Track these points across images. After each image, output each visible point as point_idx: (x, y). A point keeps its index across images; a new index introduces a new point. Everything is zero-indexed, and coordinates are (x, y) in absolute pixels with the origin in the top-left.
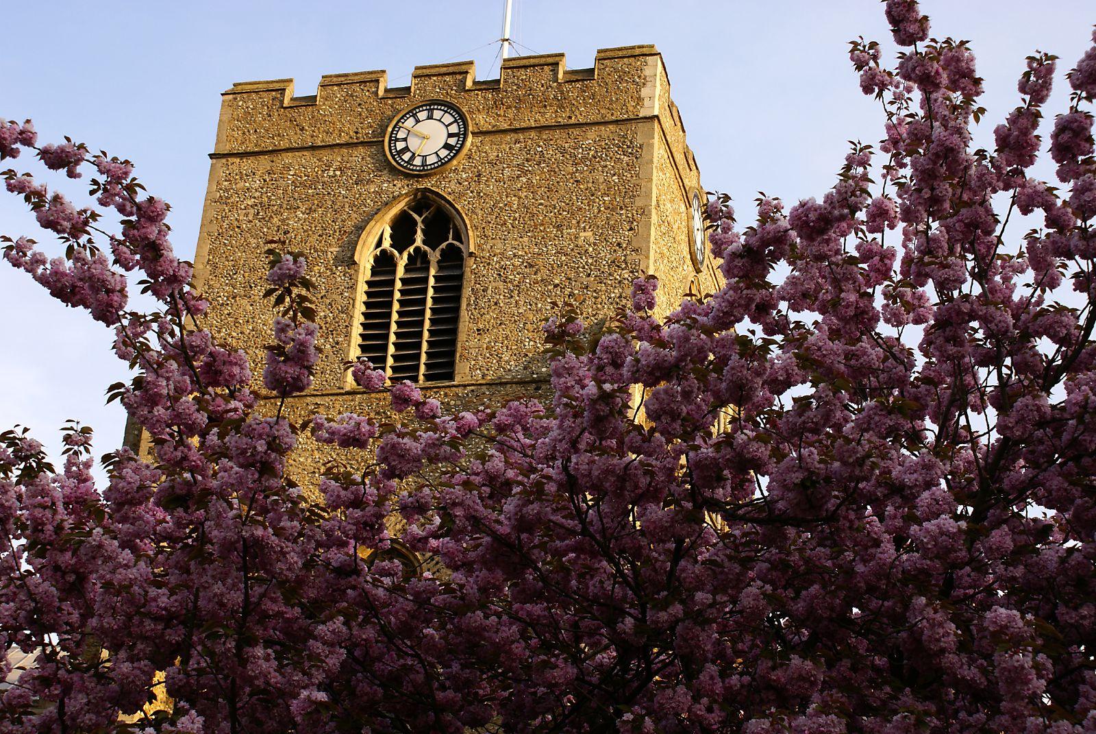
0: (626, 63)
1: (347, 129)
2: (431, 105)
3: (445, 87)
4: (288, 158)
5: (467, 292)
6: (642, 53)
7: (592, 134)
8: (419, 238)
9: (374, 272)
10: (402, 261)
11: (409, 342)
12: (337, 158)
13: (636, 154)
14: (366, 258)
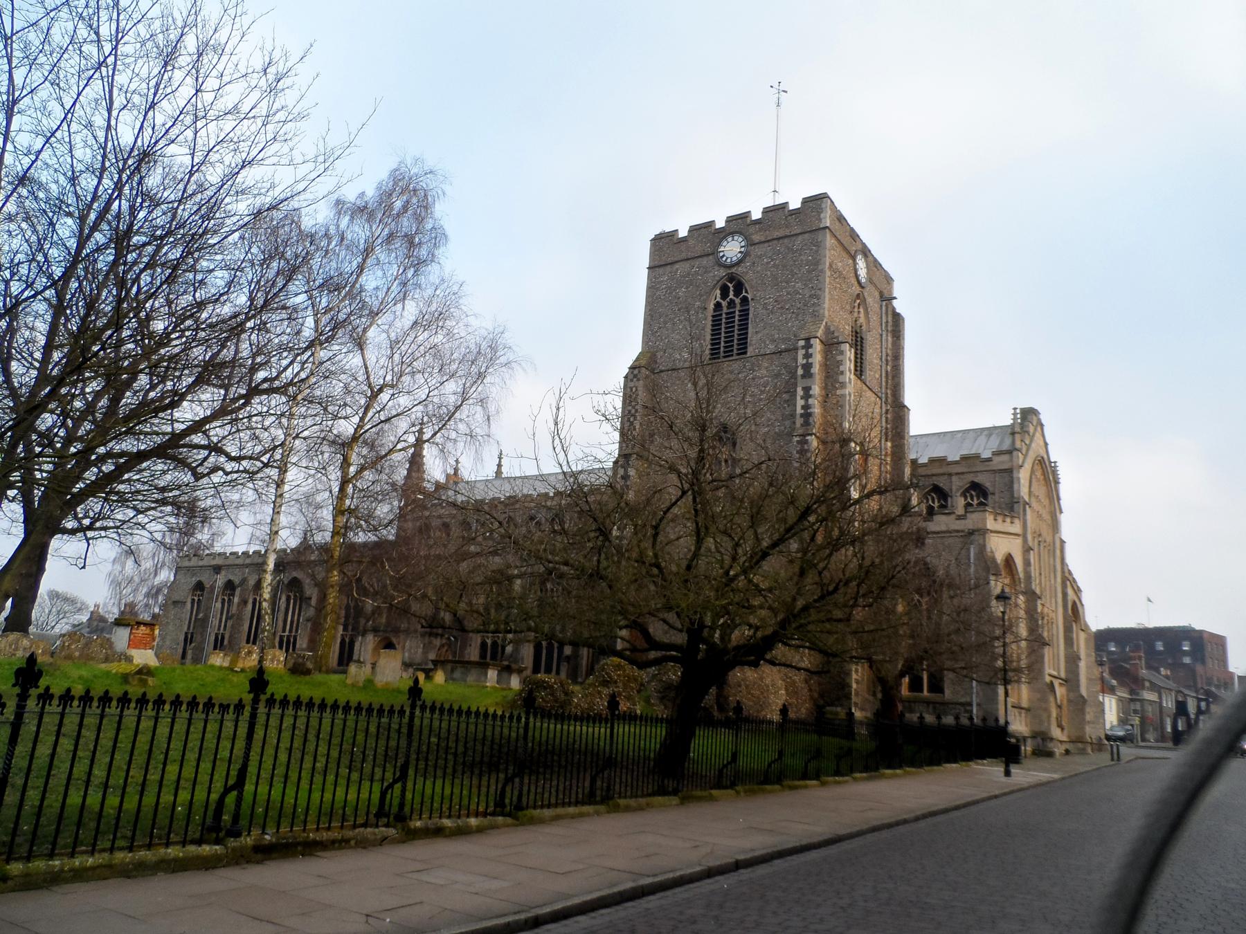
0: (816, 203)
1: (699, 250)
2: (732, 234)
3: (739, 224)
4: (677, 266)
5: (751, 316)
6: (822, 197)
7: (800, 238)
8: (731, 293)
9: (715, 310)
10: (724, 304)
11: (729, 341)
12: (697, 262)
13: (818, 245)
14: (712, 306)
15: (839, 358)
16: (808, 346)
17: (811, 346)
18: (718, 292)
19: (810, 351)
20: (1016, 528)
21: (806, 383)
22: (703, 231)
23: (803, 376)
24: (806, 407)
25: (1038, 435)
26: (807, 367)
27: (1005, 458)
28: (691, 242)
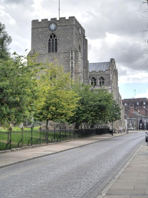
1: (44, 25)
3: (54, 20)
5: (58, 43)
7: (69, 26)
10: (51, 40)
12: (44, 29)
14: (48, 40)
15: (78, 55)
16: (72, 53)
17: (73, 53)
18: (50, 37)
19: (73, 54)
20: (110, 87)
21: (72, 61)
22: (45, 21)
23: (71, 59)
24: (72, 66)
25: (114, 65)
26: (72, 57)
27: (108, 71)
28: (42, 23)
